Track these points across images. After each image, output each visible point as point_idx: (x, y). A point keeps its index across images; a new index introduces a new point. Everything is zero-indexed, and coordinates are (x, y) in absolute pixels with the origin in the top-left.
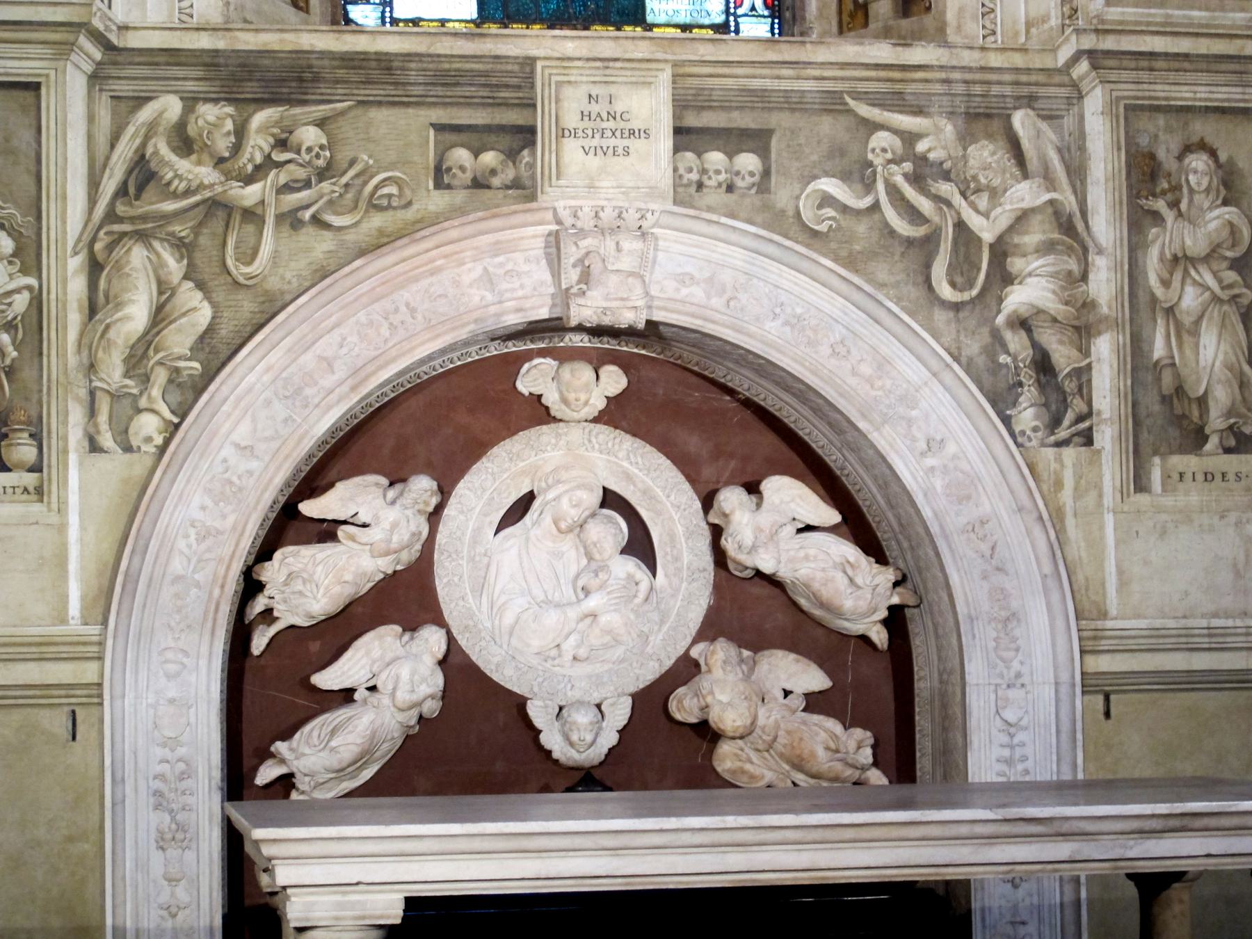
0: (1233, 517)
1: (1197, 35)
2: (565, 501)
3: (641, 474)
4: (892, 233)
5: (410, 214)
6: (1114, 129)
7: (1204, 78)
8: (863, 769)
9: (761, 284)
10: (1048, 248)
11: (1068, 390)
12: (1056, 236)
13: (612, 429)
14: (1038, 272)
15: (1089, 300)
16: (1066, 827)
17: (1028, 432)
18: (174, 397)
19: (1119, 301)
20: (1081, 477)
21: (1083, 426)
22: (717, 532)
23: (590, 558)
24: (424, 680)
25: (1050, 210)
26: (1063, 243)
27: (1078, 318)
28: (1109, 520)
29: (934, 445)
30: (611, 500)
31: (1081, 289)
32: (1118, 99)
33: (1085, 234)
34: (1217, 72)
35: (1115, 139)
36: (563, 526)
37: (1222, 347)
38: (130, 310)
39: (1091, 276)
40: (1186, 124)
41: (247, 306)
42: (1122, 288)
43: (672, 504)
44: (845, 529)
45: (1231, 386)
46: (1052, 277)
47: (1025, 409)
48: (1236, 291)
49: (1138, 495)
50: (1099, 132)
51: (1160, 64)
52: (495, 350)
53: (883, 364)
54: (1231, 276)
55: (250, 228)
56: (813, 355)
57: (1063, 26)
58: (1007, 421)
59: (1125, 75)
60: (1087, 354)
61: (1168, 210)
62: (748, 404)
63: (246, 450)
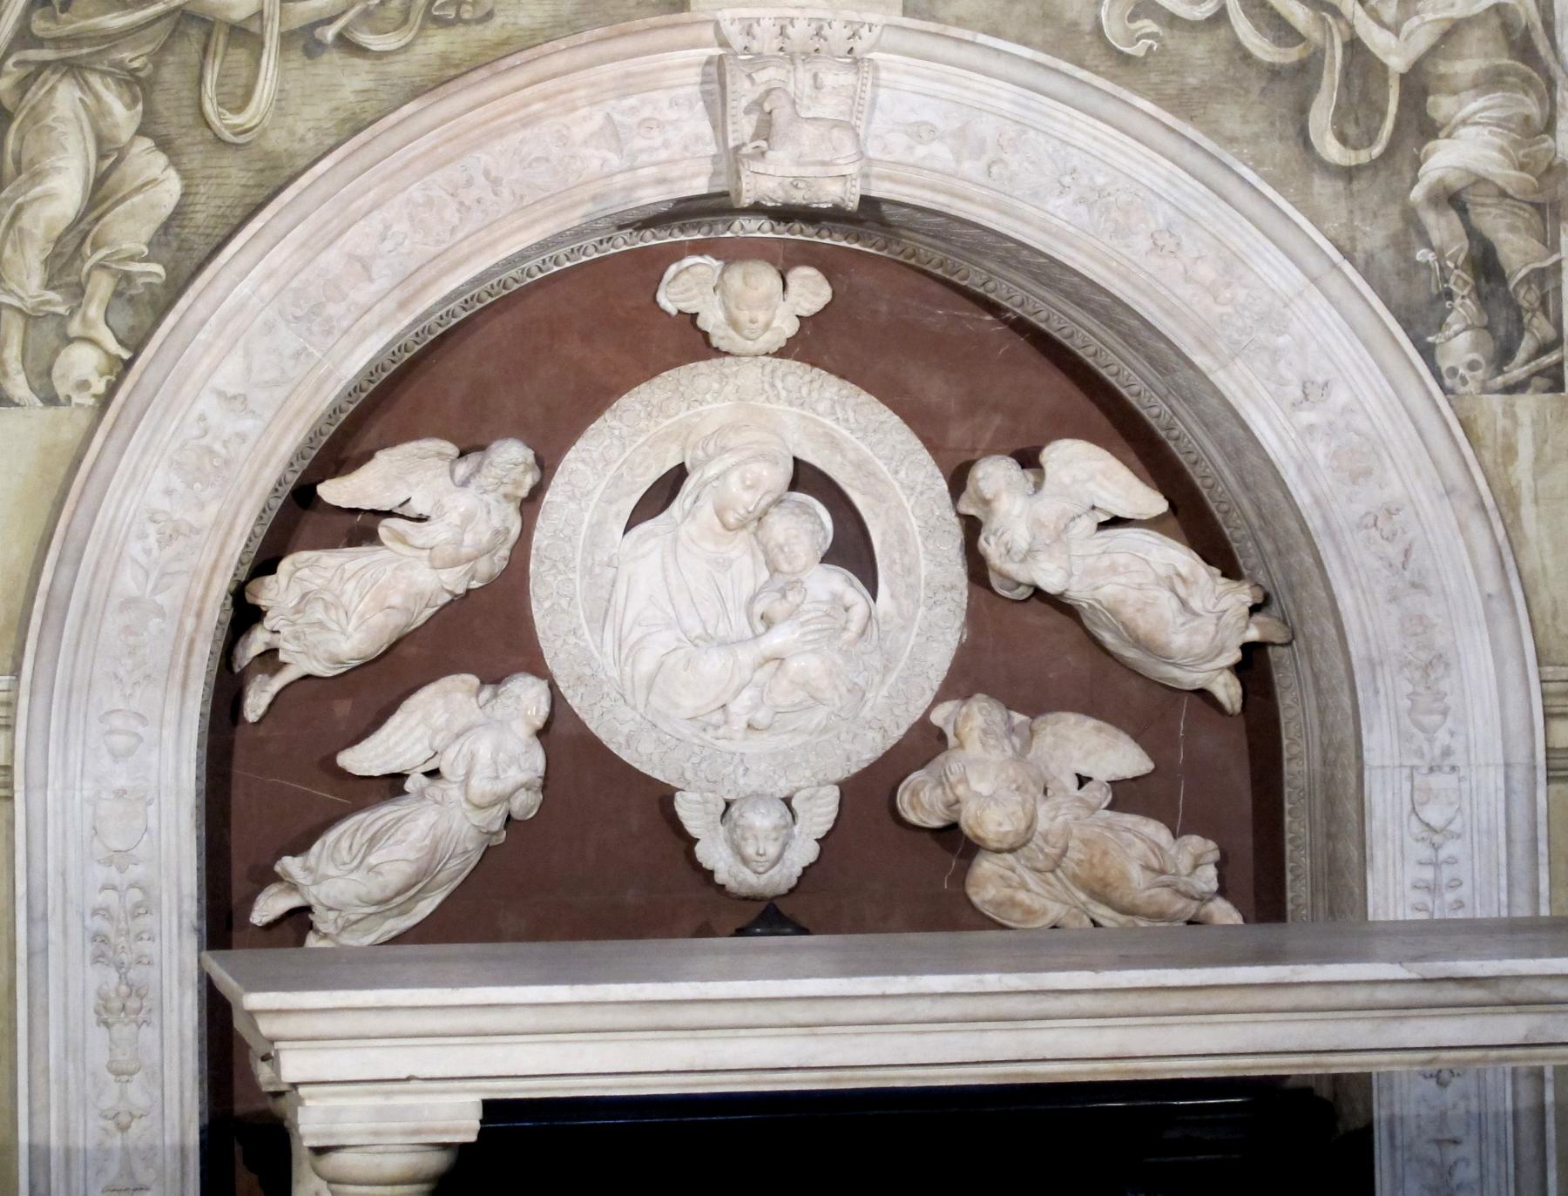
2: (734, 479)
3: (852, 438)
4: (1247, 56)
5: (490, 32)
8: (1203, 899)
9: (1041, 139)
10: (1492, 80)
11: (1525, 304)
13: (808, 367)
14: (1477, 118)
15: (1557, 161)
16: (1520, 991)
17: (1462, 371)
18: (124, 319)
20: (1545, 441)
22: (972, 527)
23: (774, 570)
24: (513, 760)
25: (1495, 22)
26: (1517, 73)
27: (1536, 191)
29: (1315, 390)
30: (806, 478)
31: (1545, 145)
36: (731, 518)
38: (53, 183)
41: (236, 176)
43: (902, 483)
44: (1173, 523)
46: (1498, 126)
47: (1456, 334)
52: (624, 243)
53: (1232, 264)
55: (240, 55)
56: (1124, 251)
58: (1428, 353)
60: (1555, 247)
62: (1022, 327)
63: (236, 401)
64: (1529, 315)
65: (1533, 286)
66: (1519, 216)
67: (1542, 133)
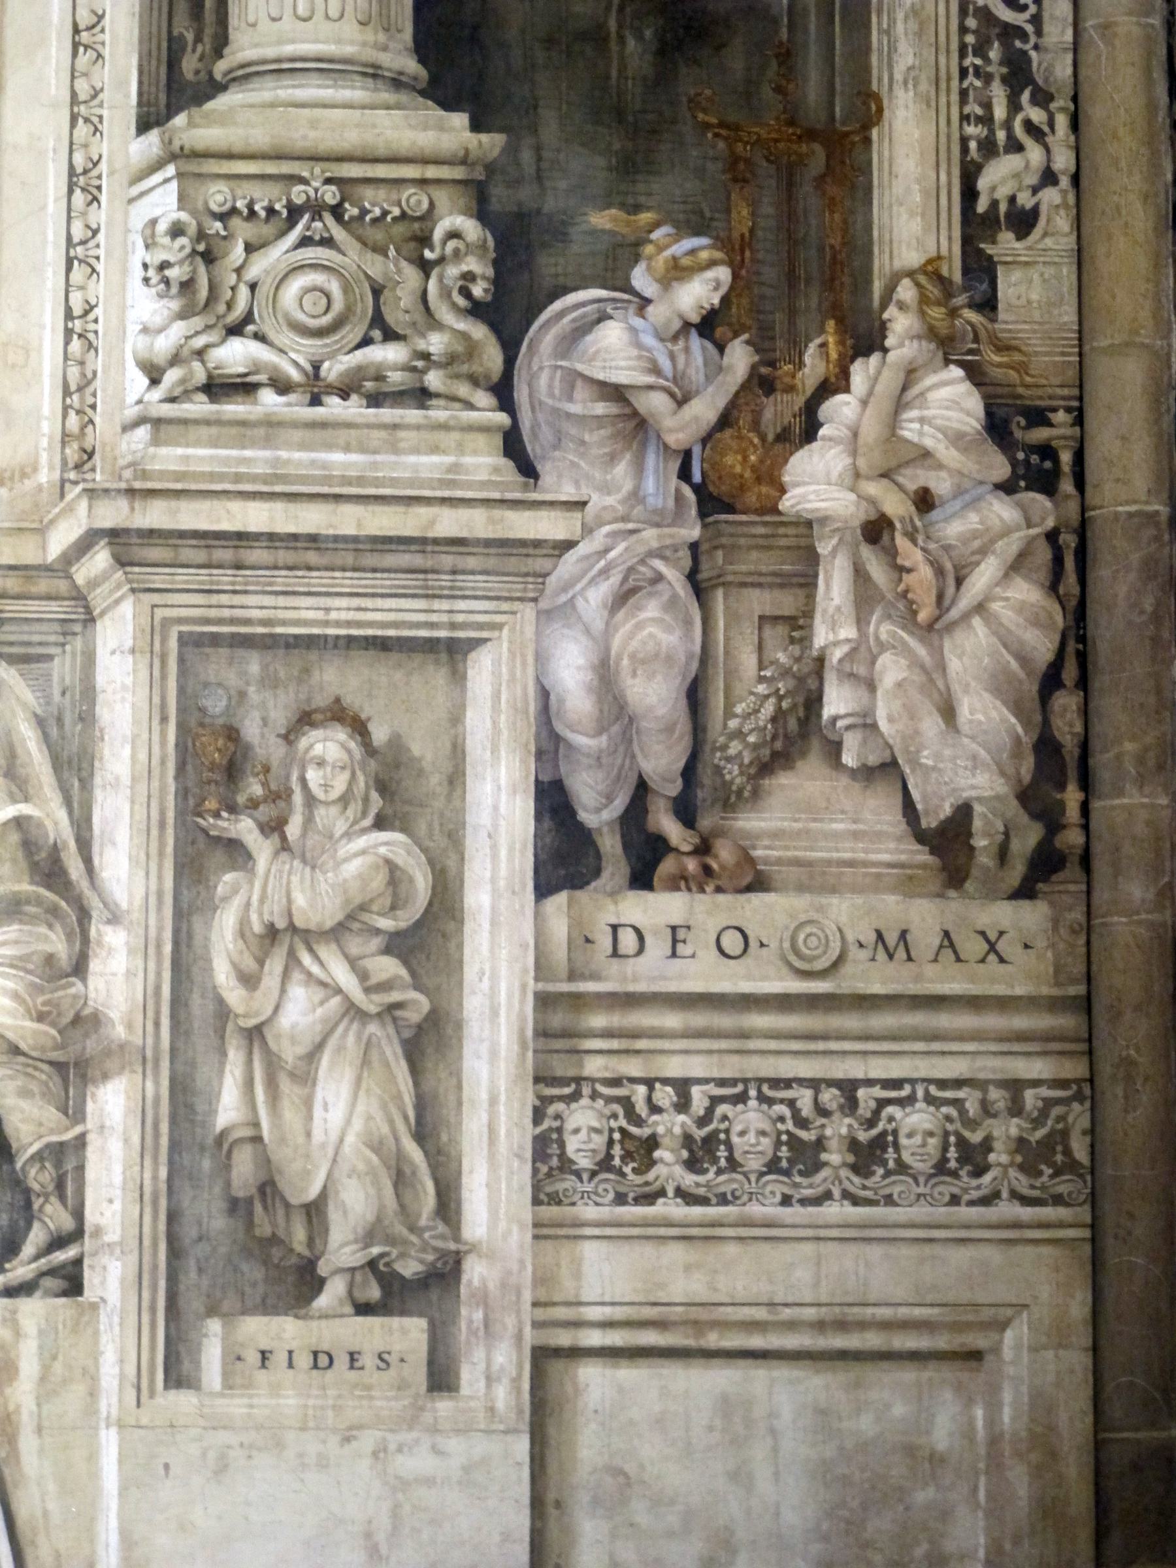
0: (367, 1440)
1: (338, 498)
6: (157, 682)
7: (345, 581)
11: (36, 1187)
12: (26, 887)
15: (87, 1011)
19: (150, 1014)
20: (54, 1358)
21: (61, 1256)
25: (14, 837)
26: (39, 901)
27: (62, 1047)
28: (110, 1442)
31: (73, 990)
32: (167, 623)
33: (84, 885)
34: (374, 570)
35: (156, 700)
37: (361, 1108)
39: (94, 966)
40: (306, 671)
42: (158, 989)
45: (376, 1183)
46: (12, 966)
48: (395, 996)
49: (173, 1395)
50: (124, 687)
51: (257, 555)
54: (387, 967)
57: (63, 482)
59: (183, 576)
60: (78, 1116)
61: (260, 838)
64: (41, 1200)
65: (47, 1165)
66: (33, 1077)
67: (67, 976)
